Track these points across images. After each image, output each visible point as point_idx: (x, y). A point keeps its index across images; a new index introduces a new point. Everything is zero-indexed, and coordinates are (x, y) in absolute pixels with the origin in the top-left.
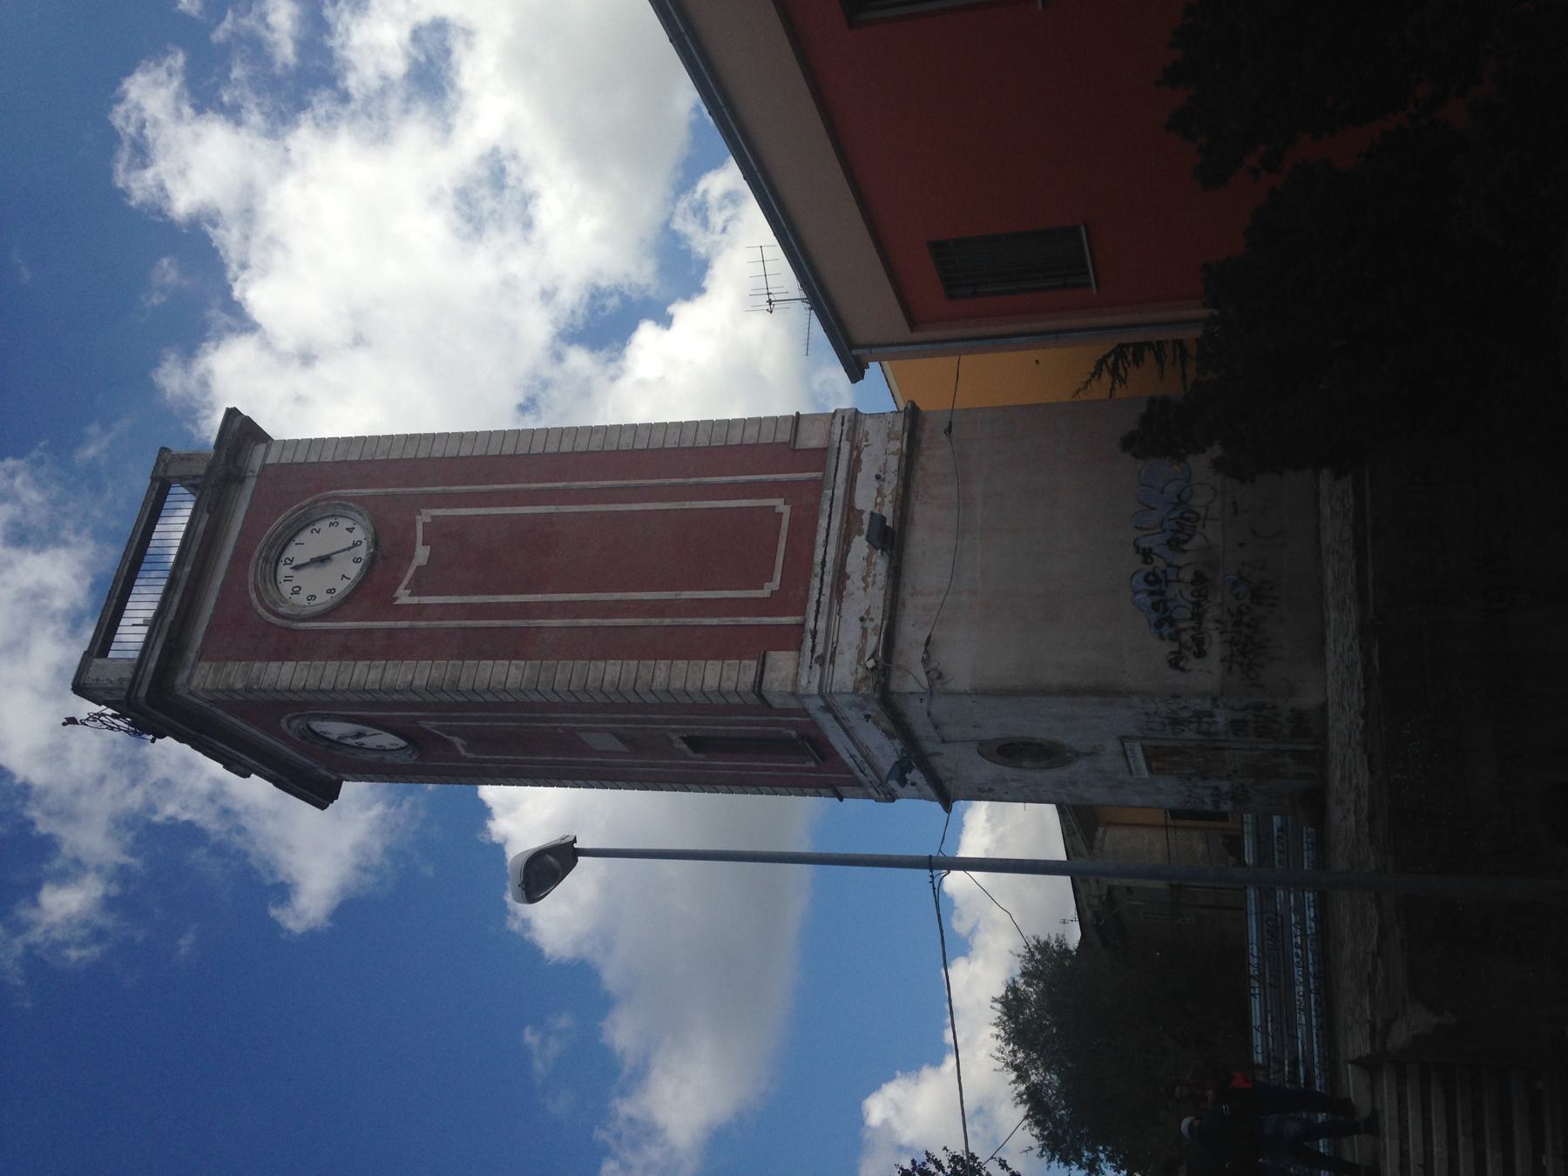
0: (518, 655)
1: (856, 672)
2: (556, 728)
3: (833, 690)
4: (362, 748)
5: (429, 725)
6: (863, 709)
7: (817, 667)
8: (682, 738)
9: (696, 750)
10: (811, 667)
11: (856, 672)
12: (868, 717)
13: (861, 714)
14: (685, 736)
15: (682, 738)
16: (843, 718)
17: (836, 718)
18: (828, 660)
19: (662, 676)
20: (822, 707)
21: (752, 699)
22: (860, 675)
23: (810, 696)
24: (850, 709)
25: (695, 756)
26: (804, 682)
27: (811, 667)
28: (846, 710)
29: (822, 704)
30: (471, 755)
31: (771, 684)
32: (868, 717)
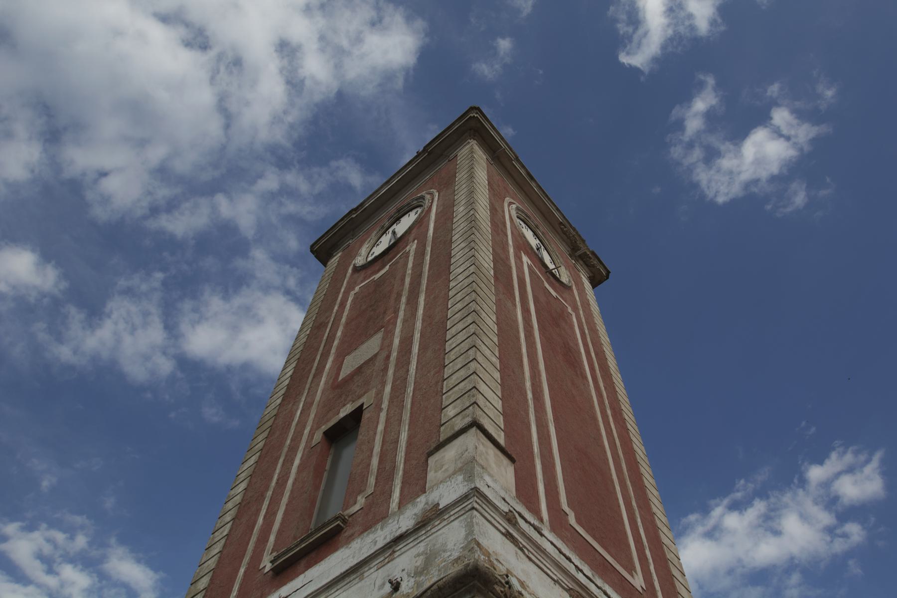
0: (496, 277)
1: (497, 560)
2: (396, 312)
3: (475, 512)
4: (374, 246)
5: (412, 247)
6: (418, 573)
7: (505, 508)
8: (362, 405)
9: (326, 434)
10: (504, 499)
11: (497, 560)
12: (396, 587)
13: (397, 575)
14: (364, 408)
15: (362, 405)
16: (394, 552)
17: (399, 539)
18: (511, 531)
19: (486, 352)
20: (438, 504)
21: (459, 424)
22: (495, 562)
23: (470, 477)
24: (418, 555)
25: (318, 436)
26: (488, 479)
27: (504, 499)
28: (421, 547)
29: (441, 507)
30: (352, 293)
31: (483, 444)
32: (396, 587)
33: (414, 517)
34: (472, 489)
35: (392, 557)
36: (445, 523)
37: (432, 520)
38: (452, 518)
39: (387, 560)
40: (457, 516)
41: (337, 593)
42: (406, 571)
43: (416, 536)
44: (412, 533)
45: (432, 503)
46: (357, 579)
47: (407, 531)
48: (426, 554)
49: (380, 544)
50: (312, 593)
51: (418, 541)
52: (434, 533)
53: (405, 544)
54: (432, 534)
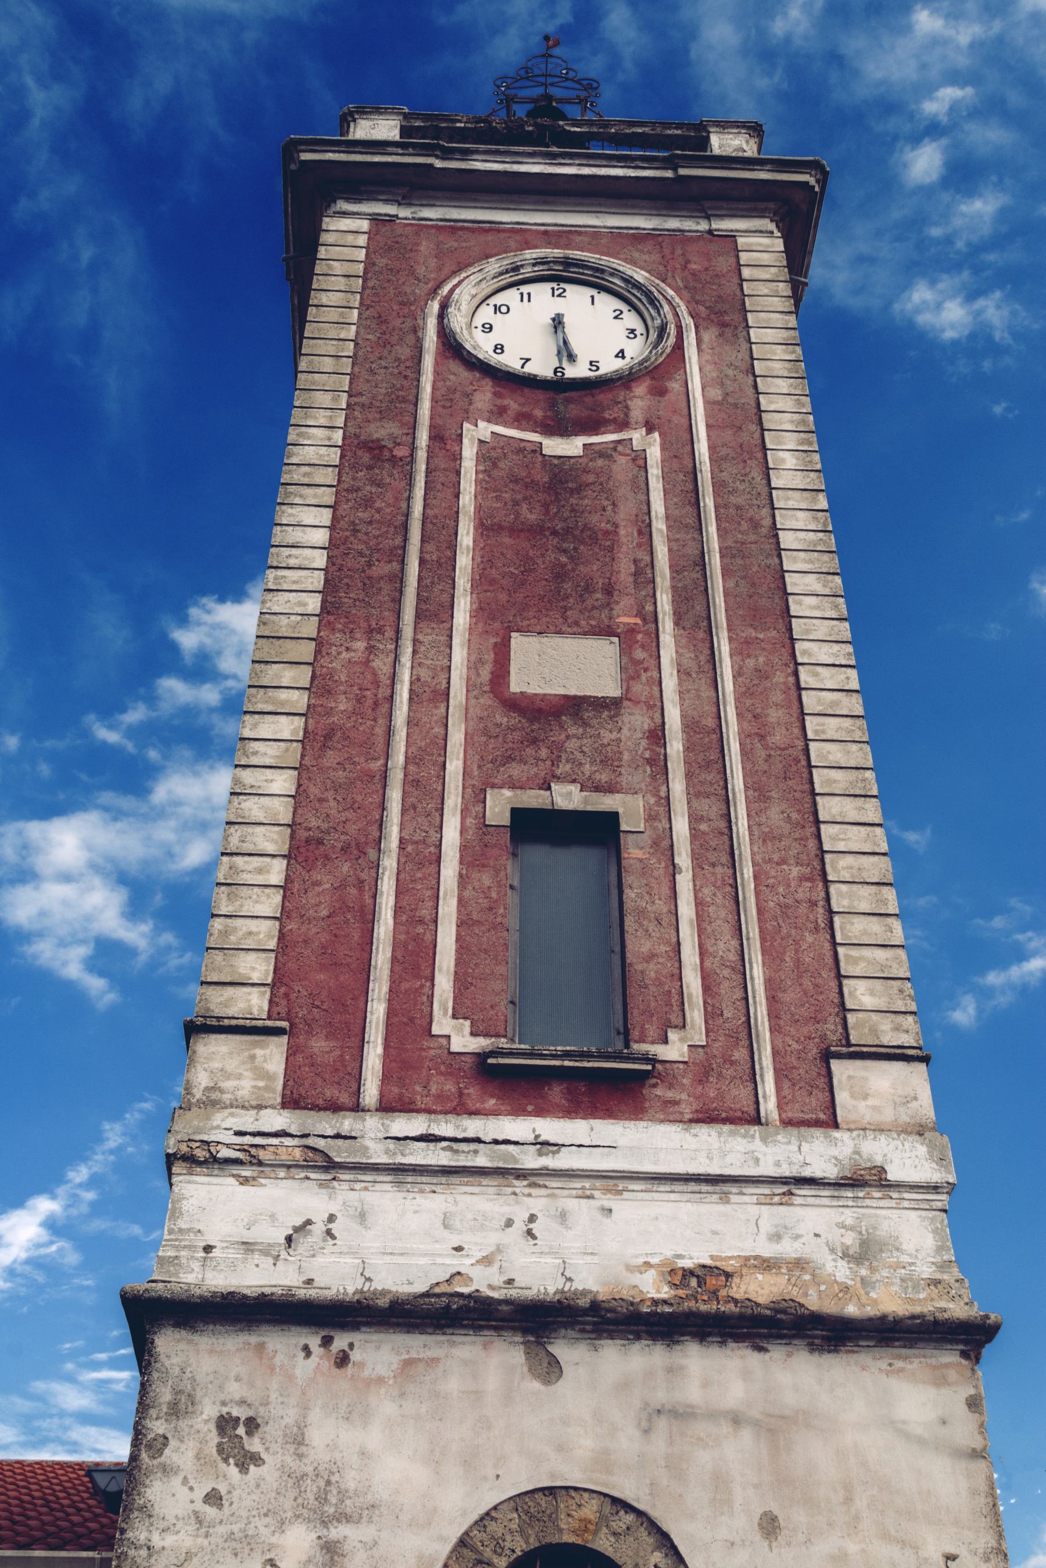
28: (848, 1216)
33: (833, 1161)
34: (948, 1183)
35: (787, 1198)
36: (892, 1203)
37: (870, 1186)
38: (906, 1204)
39: (776, 1199)
40: (913, 1205)
41: (673, 1196)
42: (823, 1239)
43: (836, 1194)
44: (829, 1184)
45: (869, 1160)
46: (715, 1196)
47: (825, 1178)
48: (860, 1233)
49: (767, 1169)
50: (624, 1172)
51: (841, 1204)
52: (872, 1207)
53: (813, 1192)
54: (867, 1207)
